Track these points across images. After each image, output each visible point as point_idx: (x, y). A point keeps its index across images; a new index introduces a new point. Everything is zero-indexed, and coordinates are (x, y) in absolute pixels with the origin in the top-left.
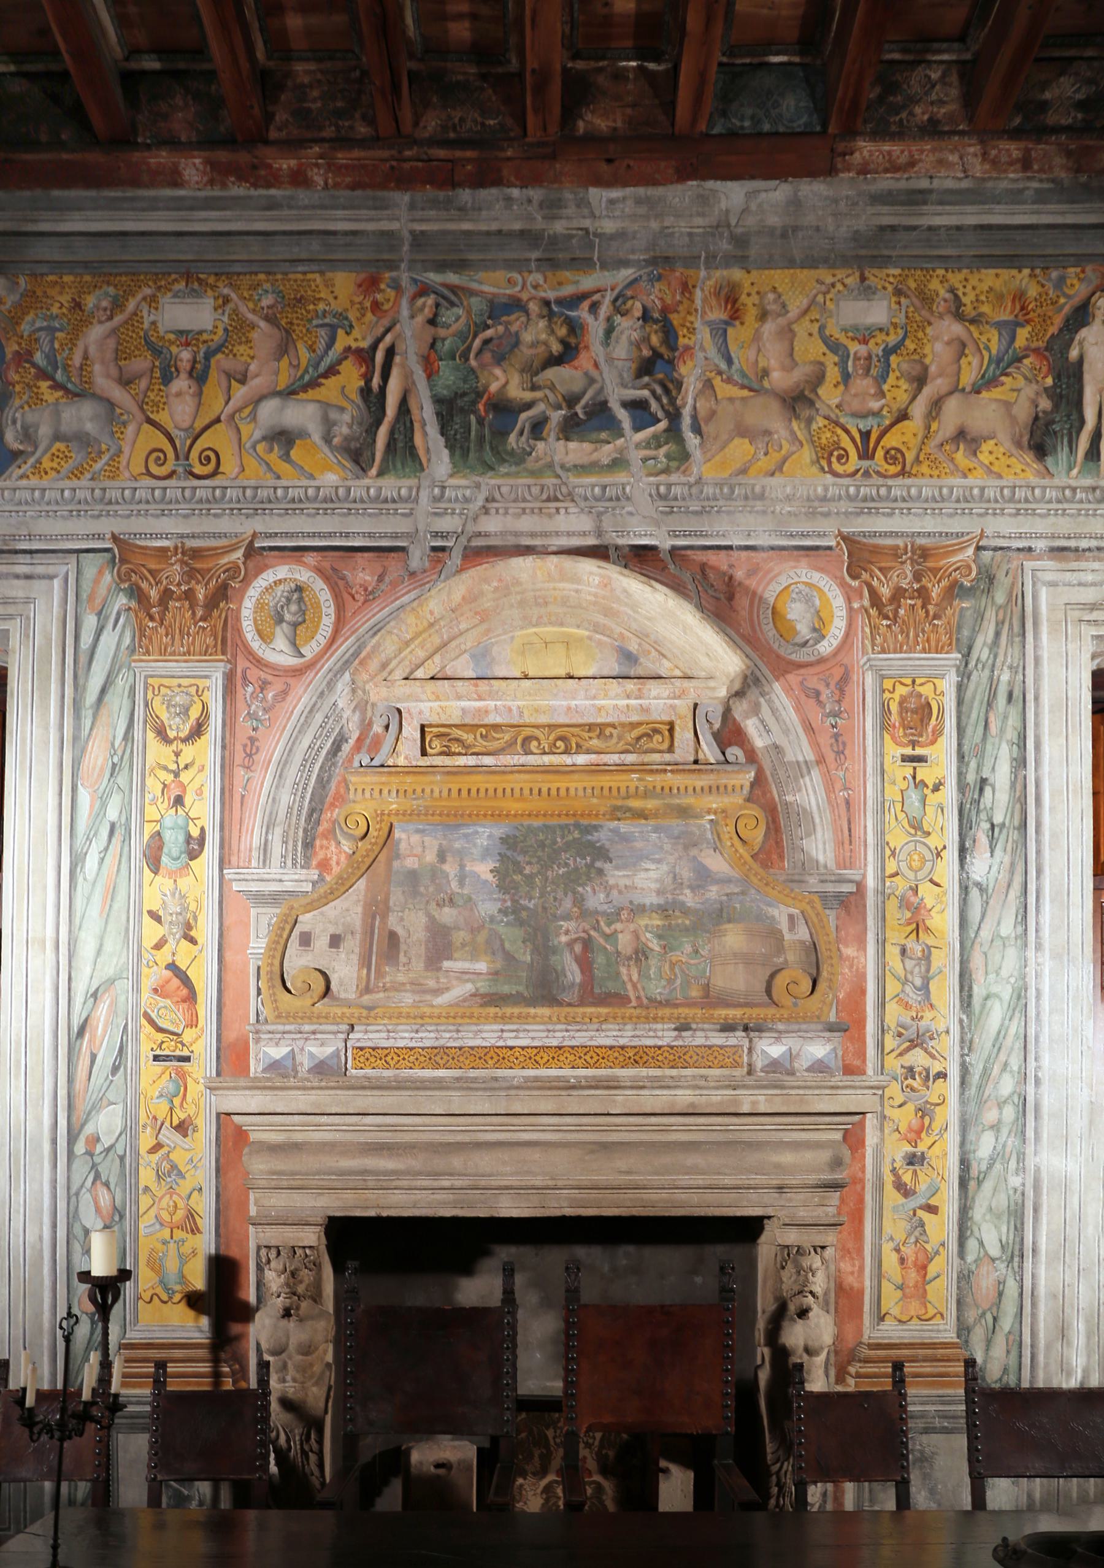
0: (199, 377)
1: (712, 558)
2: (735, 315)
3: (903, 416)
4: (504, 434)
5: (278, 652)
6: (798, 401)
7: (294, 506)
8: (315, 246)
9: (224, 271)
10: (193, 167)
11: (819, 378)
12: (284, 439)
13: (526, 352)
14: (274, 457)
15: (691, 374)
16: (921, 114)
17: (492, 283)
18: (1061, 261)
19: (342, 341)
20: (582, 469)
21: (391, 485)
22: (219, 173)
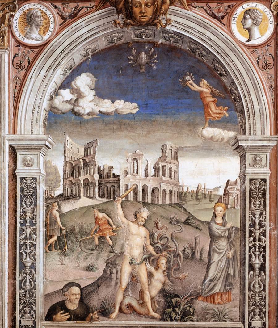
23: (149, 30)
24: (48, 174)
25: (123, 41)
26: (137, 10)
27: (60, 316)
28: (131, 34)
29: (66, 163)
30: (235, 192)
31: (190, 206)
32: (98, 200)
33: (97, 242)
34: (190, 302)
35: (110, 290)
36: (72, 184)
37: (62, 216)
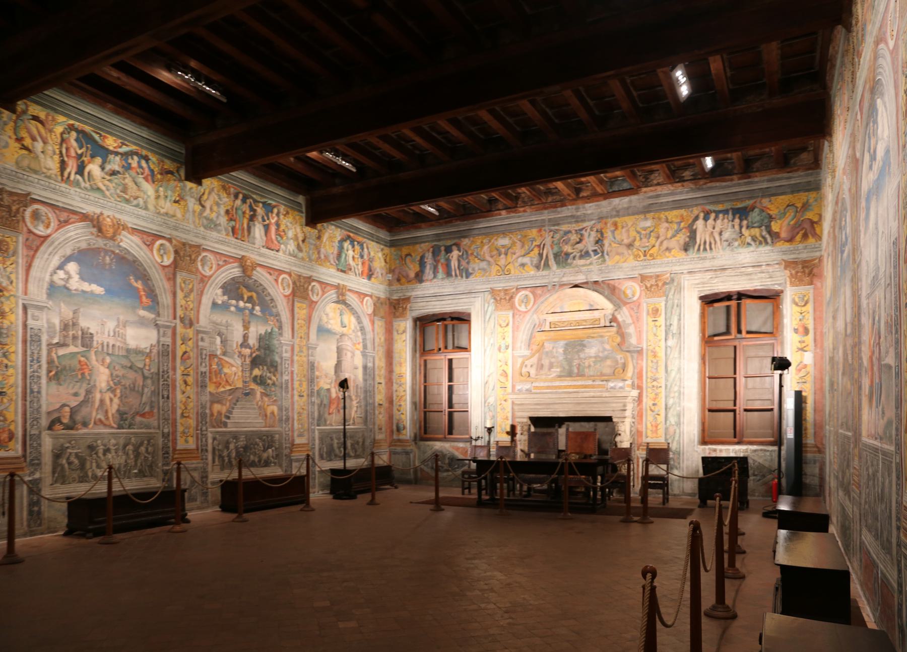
0: (506, 254)
1: (611, 282)
2: (616, 228)
3: (654, 246)
4: (567, 260)
5: (523, 308)
6: (630, 246)
7: (525, 279)
8: (528, 225)
9: (511, 232)
10: (504, 212)
11: (635, 240)
12: (523, 265)
13: (572, 242)
14: (521, 269)
15: (606, 242)
16: (655, 182)
17: (565, 228)
18: (692, 206)
19: (535, 243)
20: (583, 266)
21: (545, 273)
22: (509, 213)
23: (111, 243)
24: (49, 327)
25: (96, 246)
26: (104, 228)
27: (58, 427)
28: (100, 243)
29: (61, 321)
30: (155, 351)
31: (133, 358)
32: (80, 349)
33: (80, 377)
34: (133, 417)
35: (88, 409)
36: (65, 337)
37: (58, 357)
